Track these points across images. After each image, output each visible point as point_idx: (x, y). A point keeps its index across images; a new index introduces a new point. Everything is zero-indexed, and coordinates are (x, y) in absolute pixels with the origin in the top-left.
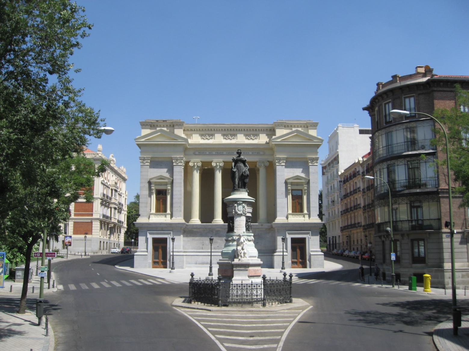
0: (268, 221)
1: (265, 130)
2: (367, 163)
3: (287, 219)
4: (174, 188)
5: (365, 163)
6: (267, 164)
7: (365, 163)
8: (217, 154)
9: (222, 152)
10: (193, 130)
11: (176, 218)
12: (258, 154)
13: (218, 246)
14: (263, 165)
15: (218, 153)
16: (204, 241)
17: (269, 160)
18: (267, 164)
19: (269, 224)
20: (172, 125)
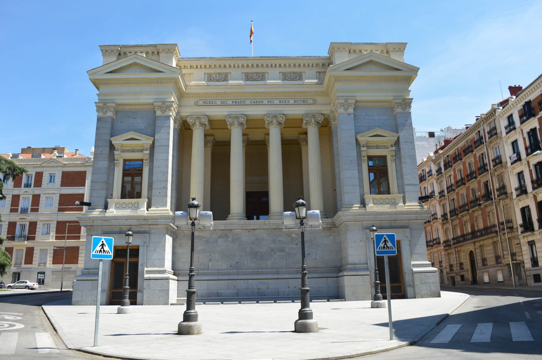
0: (325, 215)
1: (315, 65)
2: (446, 156)
3: (365, 206)
4: (156, 155)
5: (442, 156)
6: (320, 119)
7: (442, 156)
8: (234, 103)
9: (242, 101)
10: (195, 66)
11: (157, 207)
12: (304, 103)
13: (237, 263)
14: (313, 121)
15: (236, 103)
16: (211, 254)
17: (323, 112)
18: (321, 119)
19: (329, 220)
20: (156, 52)
